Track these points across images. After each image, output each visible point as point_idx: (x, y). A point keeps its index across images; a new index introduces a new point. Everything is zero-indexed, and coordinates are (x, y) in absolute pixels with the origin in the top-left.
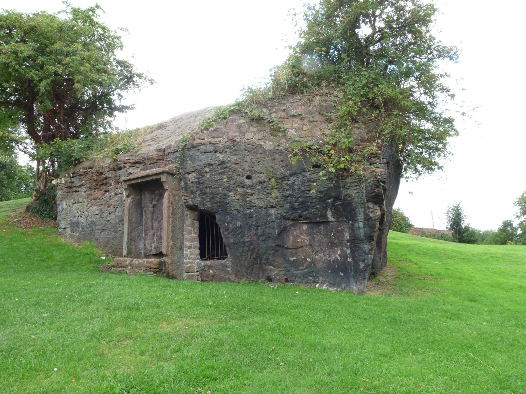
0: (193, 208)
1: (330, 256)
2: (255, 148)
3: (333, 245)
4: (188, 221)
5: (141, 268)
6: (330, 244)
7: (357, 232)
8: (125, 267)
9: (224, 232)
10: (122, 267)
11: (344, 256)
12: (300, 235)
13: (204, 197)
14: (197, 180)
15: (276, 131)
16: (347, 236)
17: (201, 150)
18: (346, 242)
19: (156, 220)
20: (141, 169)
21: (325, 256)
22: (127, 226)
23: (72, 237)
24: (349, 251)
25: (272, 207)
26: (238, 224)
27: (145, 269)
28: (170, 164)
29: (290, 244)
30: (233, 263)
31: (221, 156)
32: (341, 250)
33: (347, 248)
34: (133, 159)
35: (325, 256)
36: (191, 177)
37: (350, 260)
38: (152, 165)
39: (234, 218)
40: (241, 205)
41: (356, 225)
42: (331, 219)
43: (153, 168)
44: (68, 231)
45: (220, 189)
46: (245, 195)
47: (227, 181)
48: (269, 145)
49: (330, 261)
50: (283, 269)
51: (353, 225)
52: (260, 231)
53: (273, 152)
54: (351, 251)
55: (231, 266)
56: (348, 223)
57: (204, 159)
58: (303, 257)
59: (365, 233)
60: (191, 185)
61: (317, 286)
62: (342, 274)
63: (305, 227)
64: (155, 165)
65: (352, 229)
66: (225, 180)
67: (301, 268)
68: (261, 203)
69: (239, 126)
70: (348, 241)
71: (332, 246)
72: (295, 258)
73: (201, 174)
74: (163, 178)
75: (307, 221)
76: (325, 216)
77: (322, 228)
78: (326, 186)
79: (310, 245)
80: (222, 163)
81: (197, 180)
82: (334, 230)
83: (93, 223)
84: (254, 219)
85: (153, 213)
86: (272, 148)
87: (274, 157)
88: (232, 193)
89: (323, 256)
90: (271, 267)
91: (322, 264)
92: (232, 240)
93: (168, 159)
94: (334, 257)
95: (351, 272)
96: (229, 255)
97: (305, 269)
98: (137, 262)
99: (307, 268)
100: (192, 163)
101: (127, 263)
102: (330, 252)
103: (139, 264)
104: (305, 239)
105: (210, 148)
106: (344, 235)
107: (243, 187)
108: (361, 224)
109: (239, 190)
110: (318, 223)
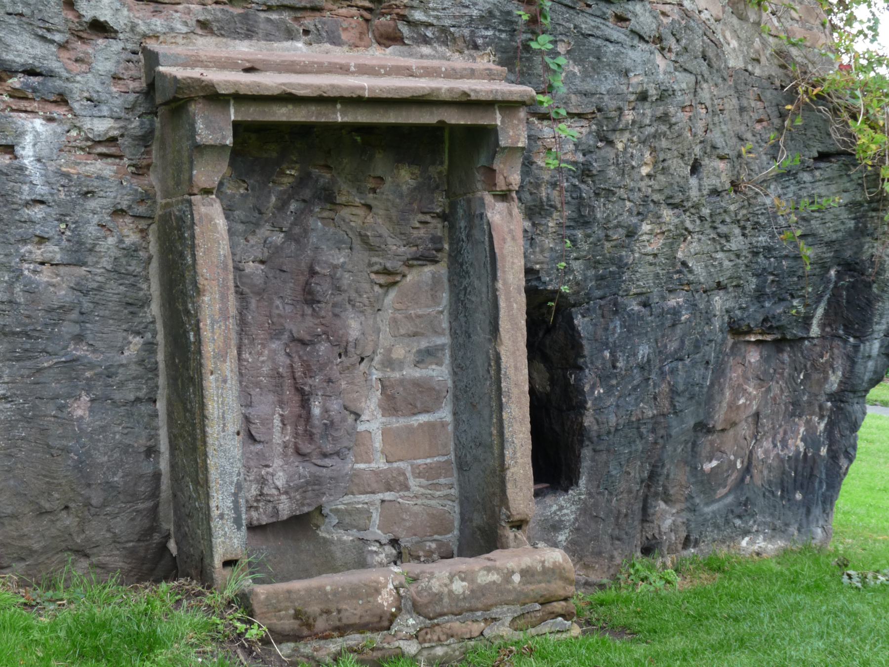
1: (785, 445)
3: (796, 409)
5: (495, 612)
6: (791, 407)
7: (859, 368)
8: (383, 623)
9: (593, 387)
10: (342, 630)
11: (811, 440)
13: (579, 234)
14: (580, 158)
16: (834, 381)
17: (633, 24)
18: (823, 398)
19: (275, 334)
20: (203, 25)
21: (775, 446)
22: (233, 382)
24: (822, 426)
25: (719, 286)
26: (644, 351)
27: (518, 609)
28: (426, 41)
29: (719, 418)
30: (584, 510)
32: (808, 422)
33: (822, 417)
35: (775, 446)
37: (824, 451)
38: (286, 16)
39: (632, 325)
40: (657, 276)
41: (864, 348)
42: (815, 330)
43: (290, 35)
45: (628, 204)
47: (649, 176)
49: (782, 460)
50: (683, 506)
51: (856, 347)
52: (680, 380)
53: (740, 82)
54: (826, 425)
55: (576, 519)
56: (846, 341)
58: (732, 457)
59: (875, 372)
60: (546, 177)
61: (744, 543)
62: (799, 496)
63: (754, 356)
64: (309, 21)
65: (851, 360)
66: (645, 171)
67: (722, 491)
70: (831, 397)
71: (793, 415)
72: (714, 463)
74: (514, 132)
75: (769, 338)
76: (806, 321)
77: (785, 357)
78: (842, 227)
79: (757, 415)
81: (580, 158)
82: (809, 364)
84: (679, 331)
85: (260, 293)
86: (740, 64)
87: (745, 103)
88: (646, 227)
89: (771, 446)
90: (662, 505)
91: (766, 472)
92: (613, 420)
93: (418, 16)
94: (793, 448)
95: (821, 487)
96: (583, 481)
97: (726, 495)
98: (459, 586)
99: (730, 491)
100: (586, 75)
101: (386, 600)
102: (785, 433)
103: (479, 592)
106: (826, 379)
107: (674, 206)
108: (876, 345)
109: (667, 214)
110: (779, 344)
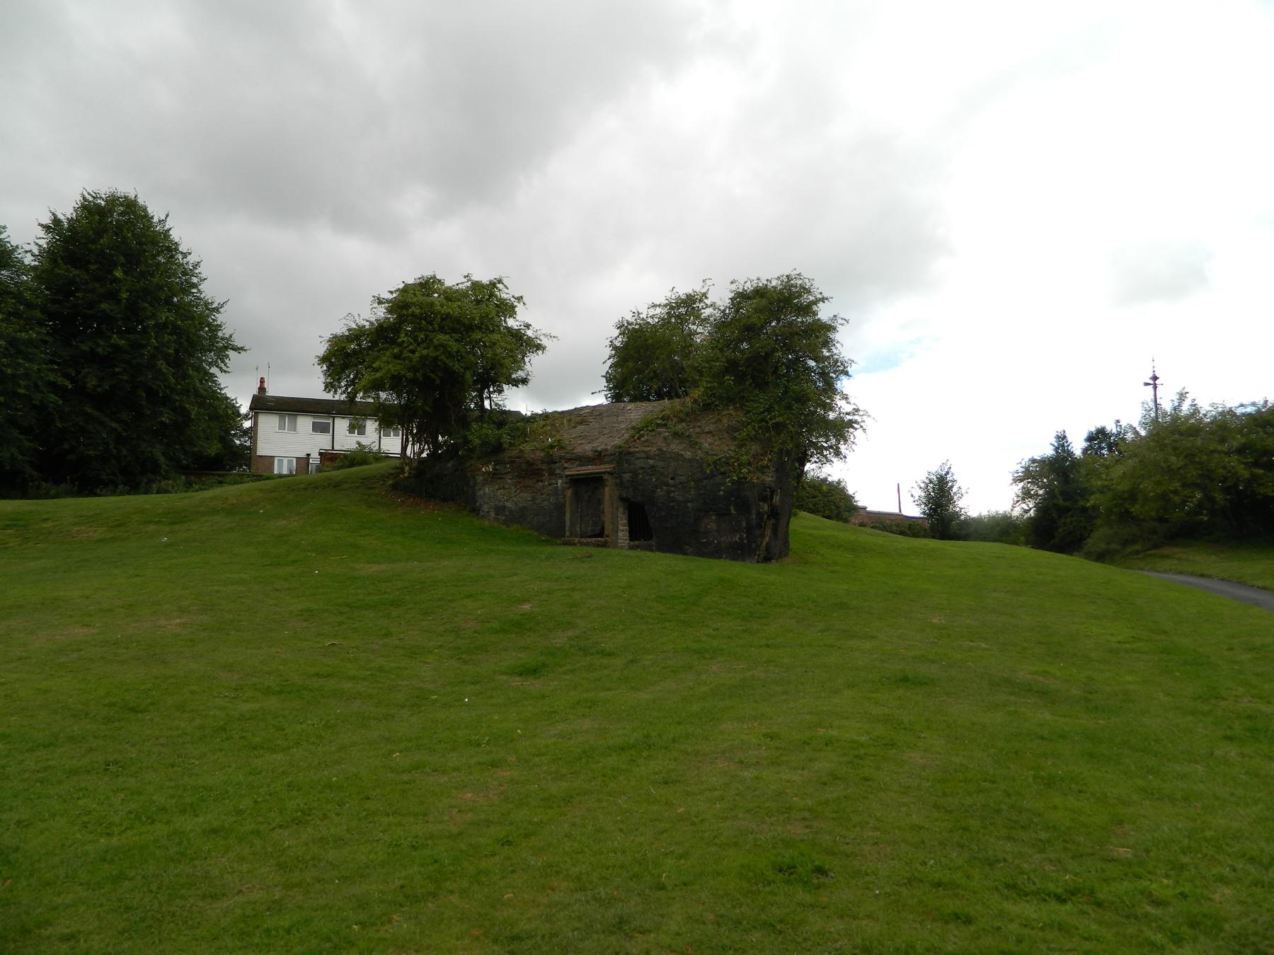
0: (622, 499)
2: (678, 457)
4: (621, 510)
12: (711, 523)
15: (693, 445)
16: (744, 524)
23: (496, 519)
31: (651, 462)
34: (568, 456)
36: (627, 476)
44: (493, 514)
46: (668, 492)
48: (688, 455)
53: (690, 461)
57: (639, 463)
68: (680, 498)
69: (665, 438)
73: (635, 473)
74: (606, 477)
80: (652, 467)
83: (524, 508)
104: (713, 526)
105: (643, 455)
